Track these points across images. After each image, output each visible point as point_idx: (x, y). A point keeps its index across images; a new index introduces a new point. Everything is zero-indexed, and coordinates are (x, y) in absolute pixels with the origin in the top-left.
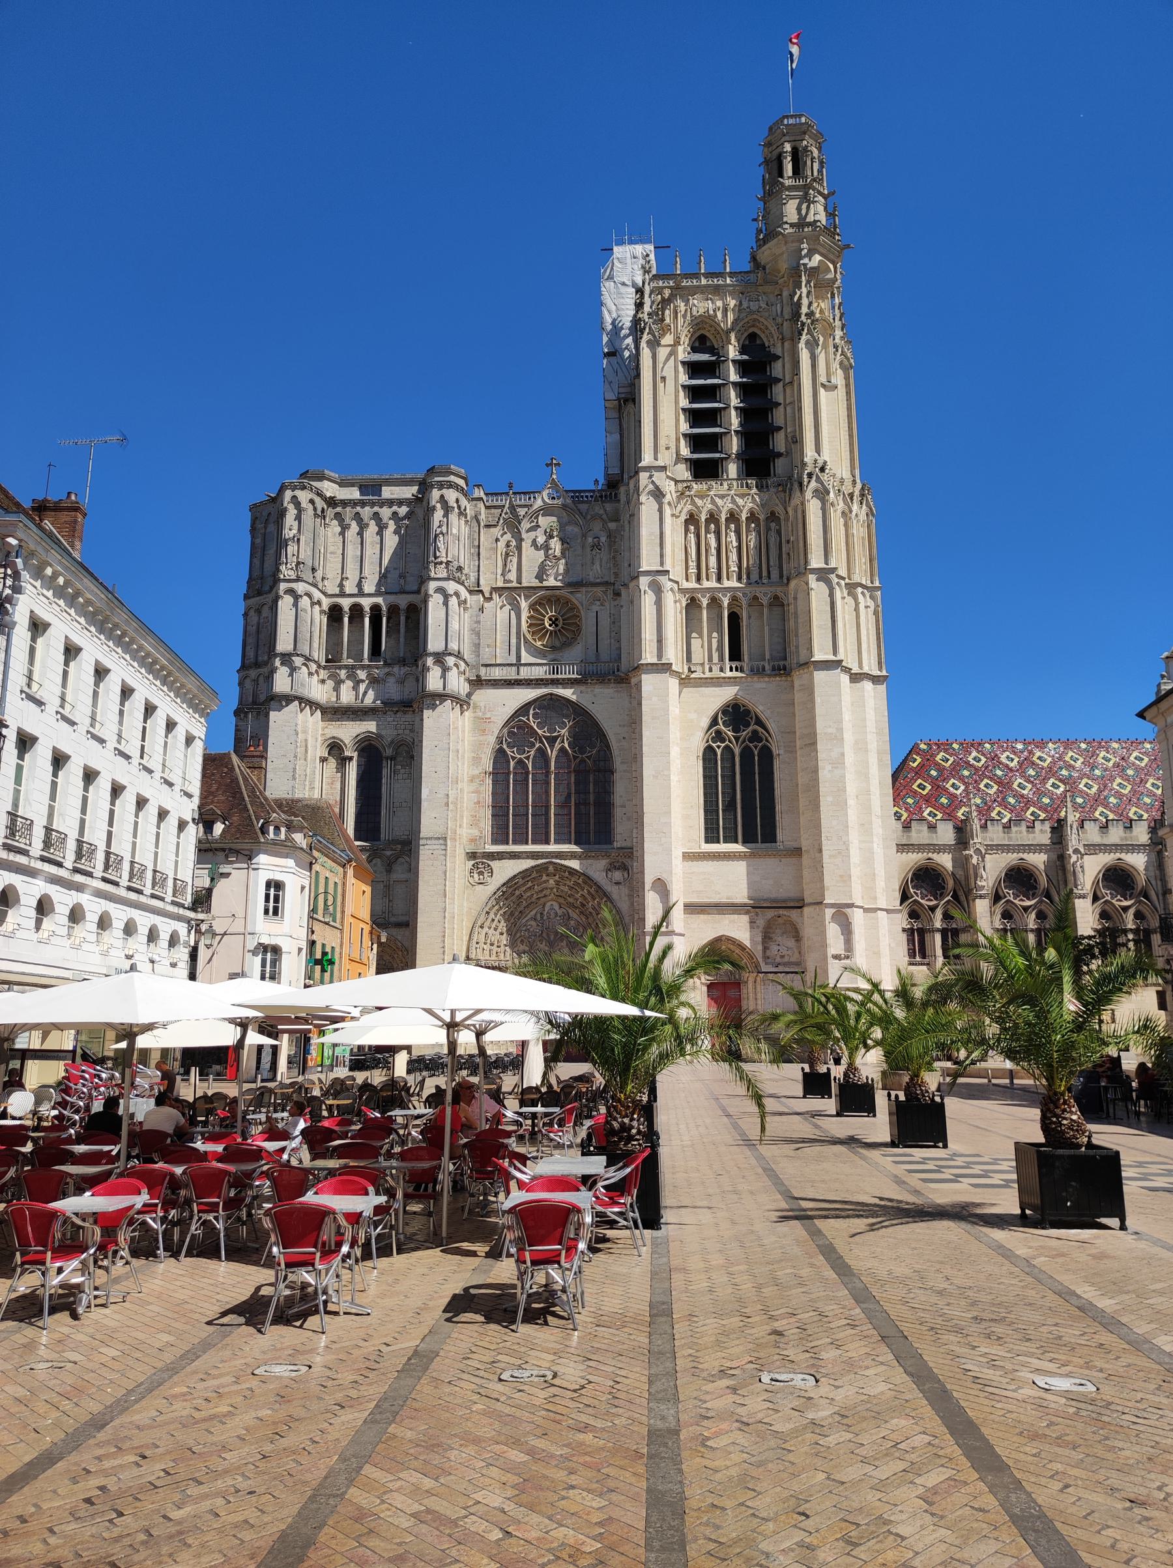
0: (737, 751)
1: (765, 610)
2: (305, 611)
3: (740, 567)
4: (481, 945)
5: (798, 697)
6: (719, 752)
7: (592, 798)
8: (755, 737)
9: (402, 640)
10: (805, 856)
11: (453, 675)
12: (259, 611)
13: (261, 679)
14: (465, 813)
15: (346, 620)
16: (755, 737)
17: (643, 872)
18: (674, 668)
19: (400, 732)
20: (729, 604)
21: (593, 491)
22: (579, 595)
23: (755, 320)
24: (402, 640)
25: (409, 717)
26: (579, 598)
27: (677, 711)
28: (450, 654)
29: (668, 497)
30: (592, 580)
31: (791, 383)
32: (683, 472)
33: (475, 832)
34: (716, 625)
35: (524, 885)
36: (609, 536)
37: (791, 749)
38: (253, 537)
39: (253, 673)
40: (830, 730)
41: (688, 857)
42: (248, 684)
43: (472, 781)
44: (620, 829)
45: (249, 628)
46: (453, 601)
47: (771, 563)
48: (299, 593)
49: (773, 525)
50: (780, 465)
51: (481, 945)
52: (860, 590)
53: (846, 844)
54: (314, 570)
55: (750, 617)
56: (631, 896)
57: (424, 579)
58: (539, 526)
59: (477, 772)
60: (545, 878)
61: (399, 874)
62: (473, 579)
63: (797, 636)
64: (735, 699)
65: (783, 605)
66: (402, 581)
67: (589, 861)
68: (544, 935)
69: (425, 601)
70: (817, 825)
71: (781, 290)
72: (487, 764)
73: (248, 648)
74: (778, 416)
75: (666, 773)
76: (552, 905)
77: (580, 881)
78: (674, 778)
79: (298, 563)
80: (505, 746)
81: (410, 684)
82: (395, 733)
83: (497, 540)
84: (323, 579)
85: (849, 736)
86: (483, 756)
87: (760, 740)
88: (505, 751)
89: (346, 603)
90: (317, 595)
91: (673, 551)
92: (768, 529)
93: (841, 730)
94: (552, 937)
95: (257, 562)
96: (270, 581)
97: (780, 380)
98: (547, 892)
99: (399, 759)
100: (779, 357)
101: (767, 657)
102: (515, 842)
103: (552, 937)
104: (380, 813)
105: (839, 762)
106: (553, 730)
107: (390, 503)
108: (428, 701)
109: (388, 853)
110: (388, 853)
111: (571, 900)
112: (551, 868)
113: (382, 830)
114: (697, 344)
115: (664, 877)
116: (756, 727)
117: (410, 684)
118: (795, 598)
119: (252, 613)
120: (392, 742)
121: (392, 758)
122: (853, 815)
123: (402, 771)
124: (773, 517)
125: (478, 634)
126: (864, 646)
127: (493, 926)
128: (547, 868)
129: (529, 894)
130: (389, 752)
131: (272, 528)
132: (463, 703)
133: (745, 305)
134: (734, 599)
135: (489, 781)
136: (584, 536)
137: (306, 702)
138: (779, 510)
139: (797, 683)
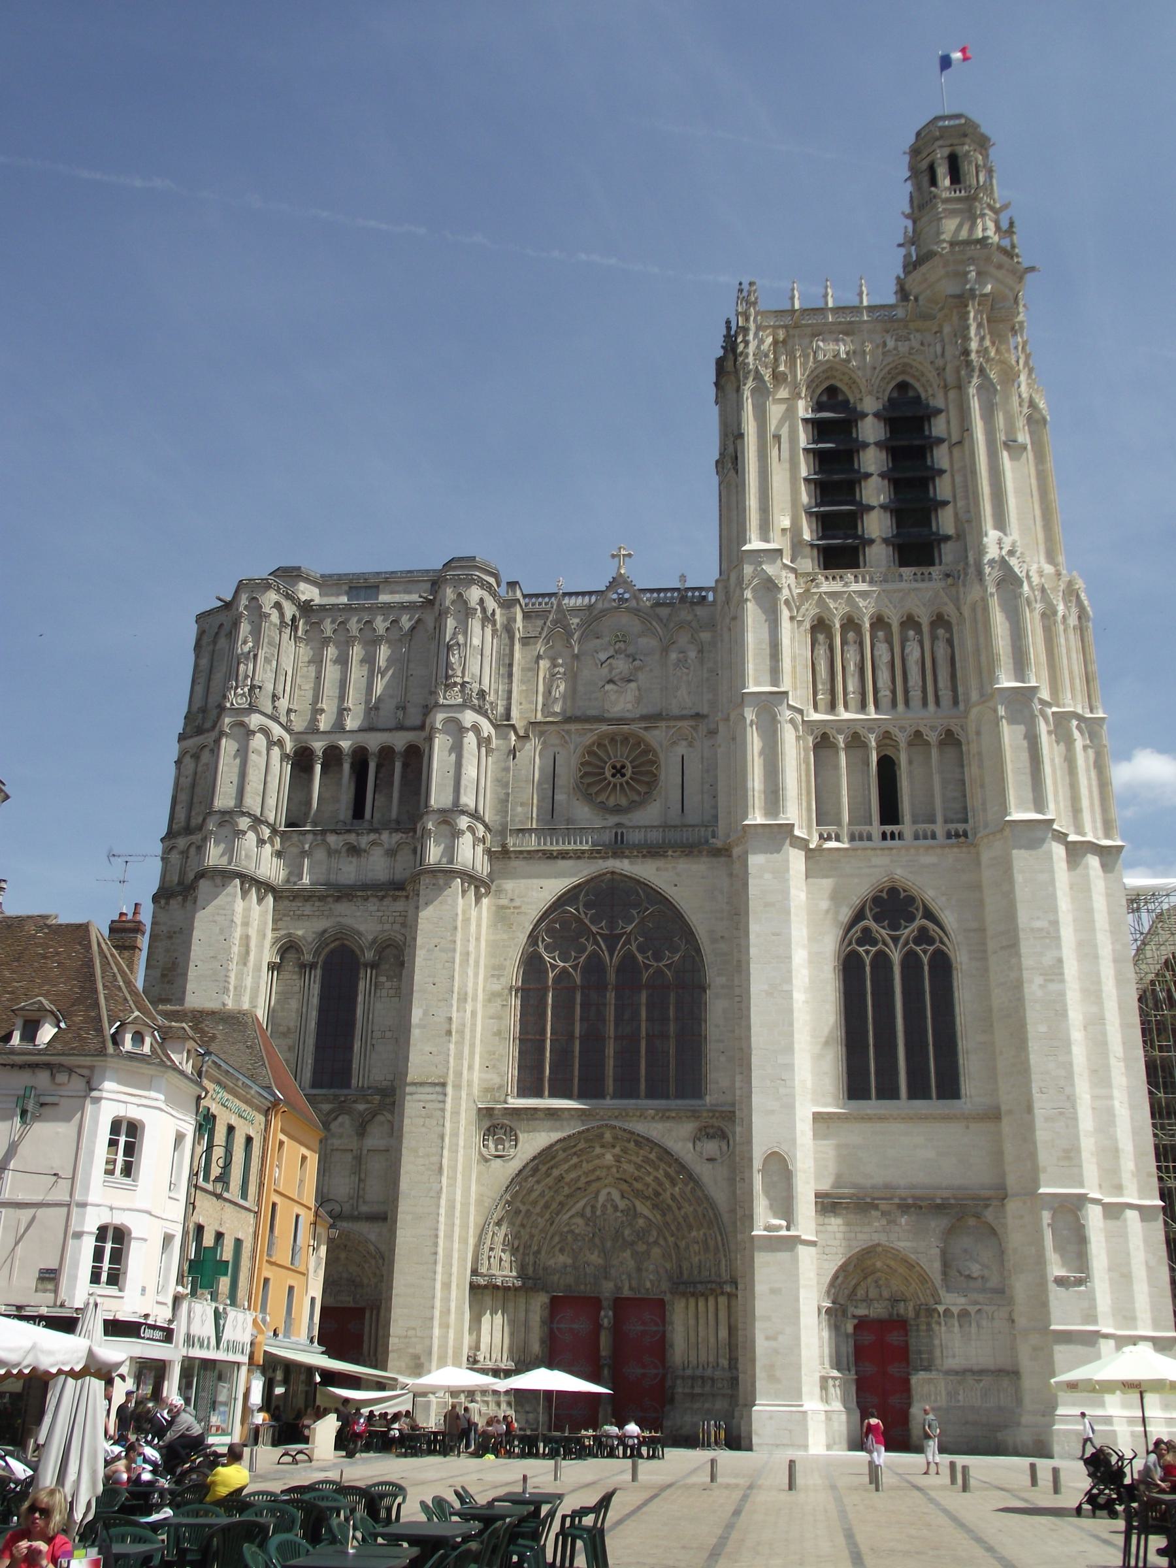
0: (896, 957)
1: (934, 752)
2: (259, 753)
3: (894, 692)
5: (987, 875)
7: (672, 1028)
8: (923, 937)
9: (396, 795)
10: (1005, 1121)
11: (465, 843)
12: (196, 757)
13: (193, 850)
14: (478, 1049)
15: (318, 768)
16: (923, 937)
17: (749, 1142)
18: (797, 832)
19: (387, 927)
21: (677, 589)
22: (656, 732)
23: (905, 365)
24: (396, 795)
25: (400, 905)
26: (656, 737)
27: (803, 896)
28: (463, 812)
29: (785, 593)
30: (675, 711)
31: (960, 443)
32: (807, 564)
34: (858, 765)
35: (566, 1160)
36: (701, 651)
37: (981, 954)
38: (197, 657)
39: (182, 842)
41: (818, 1117)
42: (175, 857)
43: (489, 1001)
44: (717, 1077)
45: (182, 779)
46: (470, 739)
47: (941, 685)
48: (252, 727)
49: (941, 632)
50: (948, 552)
53: (1071, 1100)
54: (275, 697)
55: (910, 762)
56: (732, 1181)
57: (428, 709)
59: (497, 987)
60: (598, 1150)
61: (375, 1138)
62: (501, 709)
63: (982, 786)
65: (958, 744)
66: (400, 714)
67: (668, 1125)
68: (597, 1240)
69: (430, 739)
70: (1023, 1070)
71: (941, 327)
72: (512, 974)
73: (178, 808)
74: (943, 488)
75: (786, 987)
76: (609, 1193)
77: (653, 1156)
78: (800, 997)
79: (253, 687)
80: (541, 950)
81: (404, 858)
82: (379, 928)
83: (539, 657)
84: (289, 711)
85: (1068, 934)
86: (507, 963)
87: (931, 941)
88: (541, 958)
89: (318, 746)
90: (277, 731)
91: (794, 667)
92: (934, 638)
93: (1055, 923)
94: (609, 1244)
95: (199, 689)
96: (215, 712)
97: (940, 441)
98: (603, 1173)
99: (385, 967)
100: (939, 411)
101: (939, 818)
102: (552, 1095)
103: (609, 1244)
104: (351, 1048)
105: (1055, 971)
106: (612, 925)
107: (387, 608)
108: (425, 880)
109: (361, 1107)
110: (361, 1107)
111: (638, 1186)
112: (608, 1136)
113: (355, 1072)
114: (824, 398)
115: (783, 1149)
116: (925, 922)
117: (404, 858)
118: (978, 733)
119: (187, 760)
120: (374, 941)
121: (374, 965)
122: (1079, 1054)
123: (388, 984)
124: (940, 621)
125: (506, 785)
126: (1085, 803)
127: (518, 1222)
128: (601, 1136)
129: (573, 1175)
130: (369, 955)
131: (222, 642)
132: (477, 884)
133: (891, 344)
134: (886, 738)
135: (515, 1002)
136: (665, 651)
137: (249, 881)
138: (949, 610)
139: (986, 856)
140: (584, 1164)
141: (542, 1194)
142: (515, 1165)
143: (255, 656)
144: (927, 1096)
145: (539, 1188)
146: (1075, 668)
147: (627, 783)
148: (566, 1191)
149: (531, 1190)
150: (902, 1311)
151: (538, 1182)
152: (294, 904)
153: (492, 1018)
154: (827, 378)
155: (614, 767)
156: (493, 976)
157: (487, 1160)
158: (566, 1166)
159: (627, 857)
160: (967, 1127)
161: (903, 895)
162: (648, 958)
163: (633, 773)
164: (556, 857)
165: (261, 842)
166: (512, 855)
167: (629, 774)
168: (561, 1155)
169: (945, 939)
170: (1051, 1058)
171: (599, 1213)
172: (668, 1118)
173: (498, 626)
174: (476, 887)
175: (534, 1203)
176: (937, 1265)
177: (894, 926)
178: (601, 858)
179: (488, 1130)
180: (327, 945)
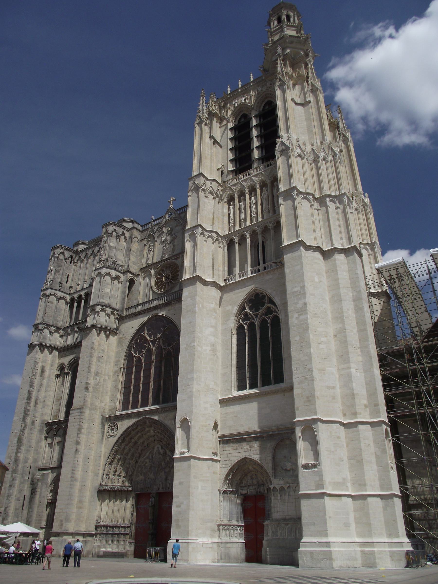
0: (257, 323)
4: (111, 476)
6: (246, 327)
8: (269, 311)
16: (269, 311)
20: (251, 236)
33: (113, 404)
40: (295, 290)
41: (224, 402)
51: (111, 476)
52: (328, 199)
58: (163, 232)
59: (117, 369)
60: (147, 429)
64: (254, 290)
67: (166, 414)
83: (145, 245)
86: (120, 359)
89: (76, 296)
129: (141, 441)
140: (144, 436)
141: (130, 450)
142: (116, 438)
143: (52, 271)
144: (269, 384)
145: (127, 448)
146: (331, 177)
147: (171, 282)
148: (140, 448)
149: (124, 449)
150: (262, 491)
151: (126, 445)
152: (64, 353)
153: (114, 381)
154: (240, 112)
155: (166, 277)
156: (116, 365)
157: (108, 438)
158: (136, 437)
159: (159, 308)
160: (284, 395)
161: (260, 295)
162: (165, 346)
163: (172, 277)
164: (138, 315)
165: (51, 333)
166: (125, 318)
167: (170, 277)
168: (133, 433)
169: (277, 310)
170: (301, 352)
171: (154, 456)
172: (166, 411)
173: (128, 238)
174: (105, 332)
175: (127, 454)
176: (270, 465)
177: (257, 310)
178: (152, 311)
179: (109, 425)
180: (72, 365)
